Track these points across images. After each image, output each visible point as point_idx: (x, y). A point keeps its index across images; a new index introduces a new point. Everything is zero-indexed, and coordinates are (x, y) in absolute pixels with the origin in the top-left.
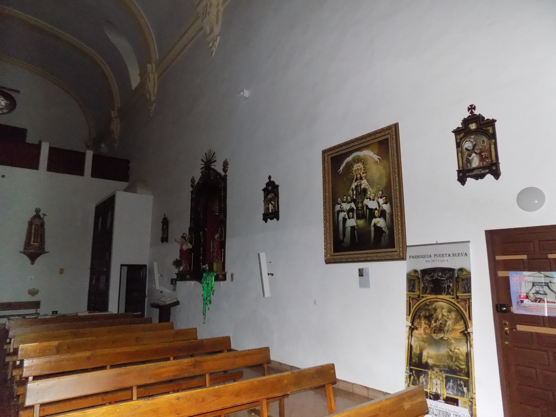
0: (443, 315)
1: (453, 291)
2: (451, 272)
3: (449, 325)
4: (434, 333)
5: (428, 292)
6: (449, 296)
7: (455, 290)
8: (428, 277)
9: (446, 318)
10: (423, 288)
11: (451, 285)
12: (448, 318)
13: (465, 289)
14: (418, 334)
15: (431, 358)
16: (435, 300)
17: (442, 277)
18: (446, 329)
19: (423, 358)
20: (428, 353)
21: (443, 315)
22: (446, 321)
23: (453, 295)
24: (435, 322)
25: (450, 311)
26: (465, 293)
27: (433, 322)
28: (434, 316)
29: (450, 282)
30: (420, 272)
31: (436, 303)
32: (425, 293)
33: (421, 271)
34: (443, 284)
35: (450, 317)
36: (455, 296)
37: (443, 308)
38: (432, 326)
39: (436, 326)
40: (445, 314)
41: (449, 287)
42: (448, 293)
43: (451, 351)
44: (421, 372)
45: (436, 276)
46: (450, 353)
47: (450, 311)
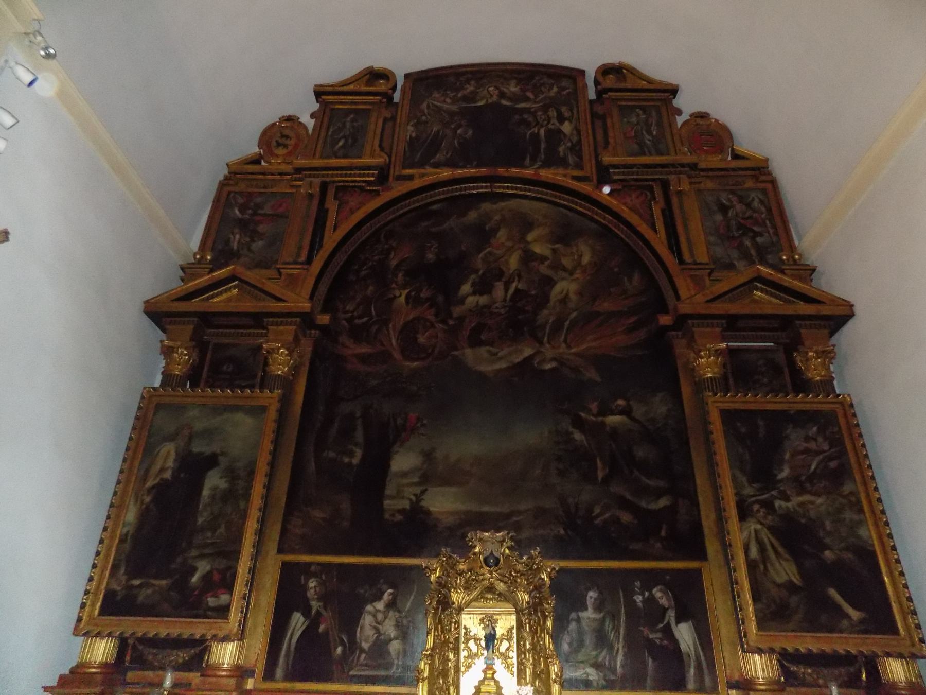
0: (528, 257)
1: (576, 149)
2: (565, 83)
3: (564, 300)
4: (475, 342)
5: (439, 157)
6: (561, 171)
7: (587, 151)
8: (446, 103)
9: (544, 269)
10: (412, 142)
11: (567, 128)
12: (557, 266)
13: (641, 145)
14: (364, 359)
15: (446, 482)
16: (483, 188)
17: (515, 99)
18: (547, 316)
19: (390, 490)
20: (428, 456)
21: (528, 257)
22: (549, 282)
23: (579, 166)
24: (483, 287)
25: (564, 235)
26: (644, 154)
27: (466, 288)
28: (479, 261)
29: (561, 119)
30: (400, 83)
31: (486, 206)
32: (421, 165)
33: (407, 76)
34: (528, 125)
35: (566, 262)
36: (590, 169)
37: (526, 224)
38: (457, 311)
39: (480, 311)
40: (538, 249)
41: (555, 136)
42: (553, 160)
43: (579, 424)
44: (373, 575)
45: (489, 94)
46: (578, 436)
47: (564, 235)
